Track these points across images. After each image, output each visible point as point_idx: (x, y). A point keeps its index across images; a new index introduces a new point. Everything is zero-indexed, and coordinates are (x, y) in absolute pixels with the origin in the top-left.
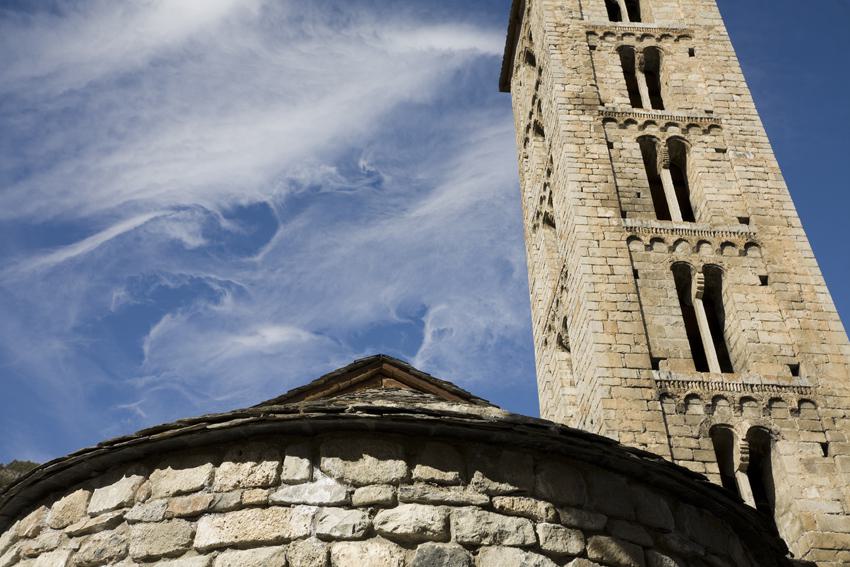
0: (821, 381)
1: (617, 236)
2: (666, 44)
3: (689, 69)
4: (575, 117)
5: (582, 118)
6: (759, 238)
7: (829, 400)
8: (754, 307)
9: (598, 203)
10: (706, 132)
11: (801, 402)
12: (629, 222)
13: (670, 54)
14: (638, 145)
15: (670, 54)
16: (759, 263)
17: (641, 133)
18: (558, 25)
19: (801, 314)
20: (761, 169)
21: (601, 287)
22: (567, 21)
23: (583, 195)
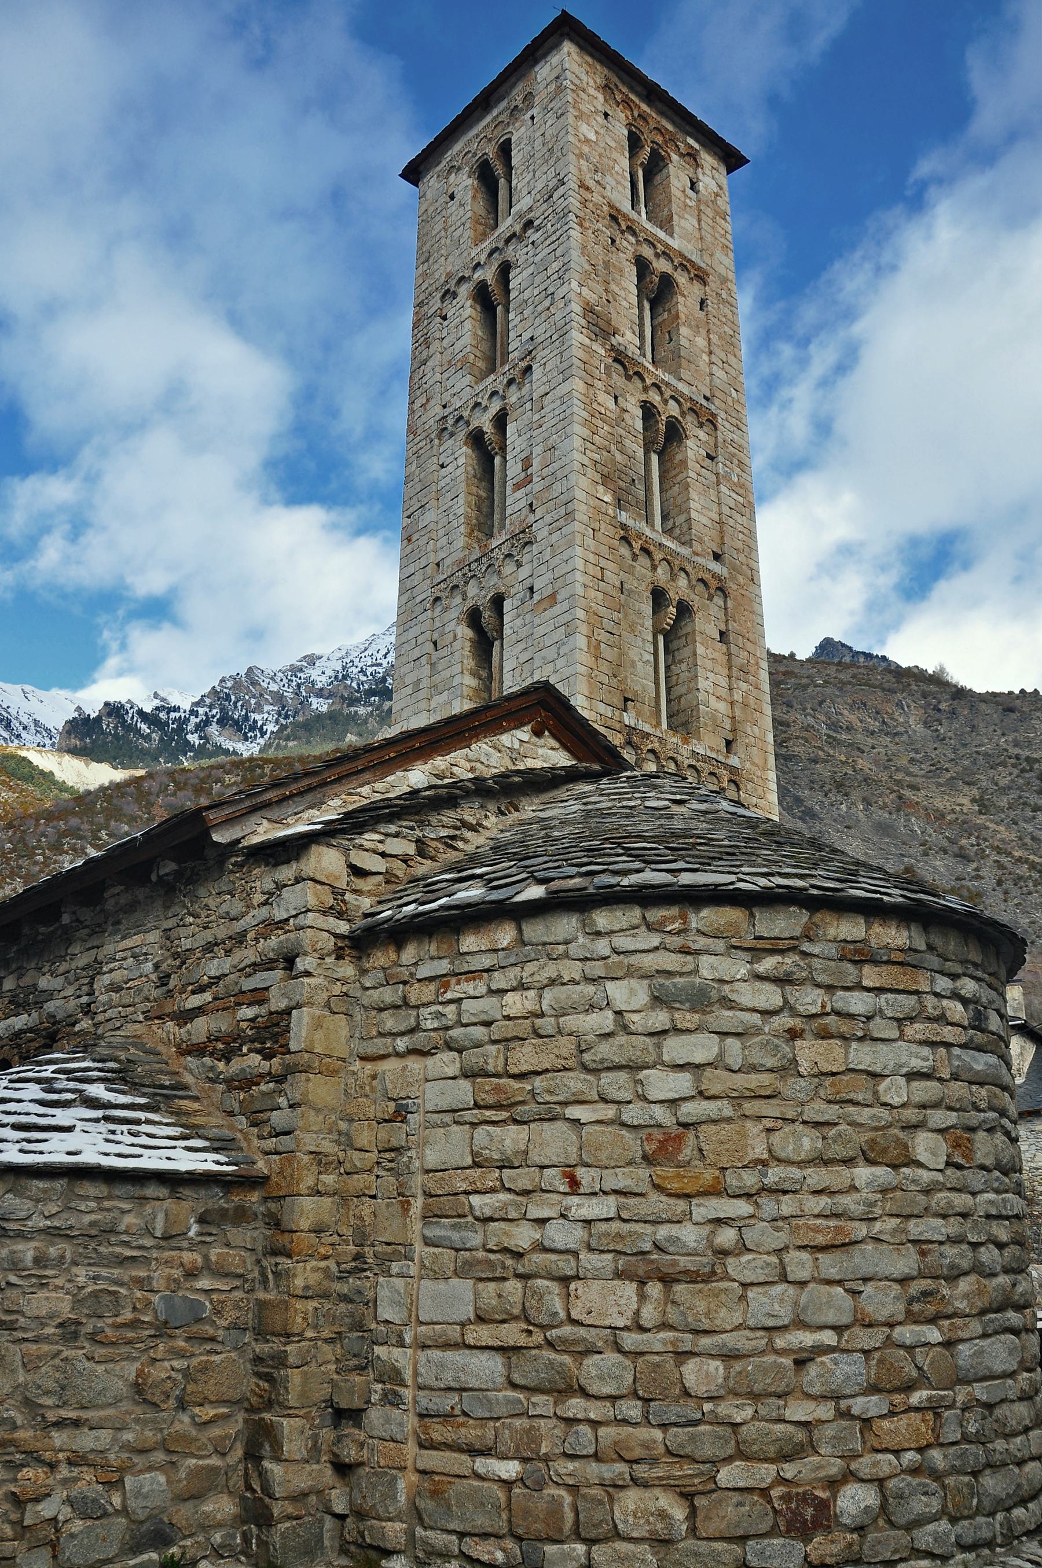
0: (748, 765)
1: (611, 531)
2: (681, 279)
3: (698, 327)
4: (587, 341)
5: (596, 346)
6: (731, 586)
7: (750, 786)
8: (709, 664)
9: (598, 477)
10: (701, 425)
11: (731, 781)
12: (624, 517)
13: (683, 295)
14: (639, 412)
15: (683, 295)
16: (721, 615)
17: (644, 397)
18: (583, 186)
19: (744, 686)
20: (741, 499)
21: (592, 594)
22: (591, 184)
23: (586, 462)
